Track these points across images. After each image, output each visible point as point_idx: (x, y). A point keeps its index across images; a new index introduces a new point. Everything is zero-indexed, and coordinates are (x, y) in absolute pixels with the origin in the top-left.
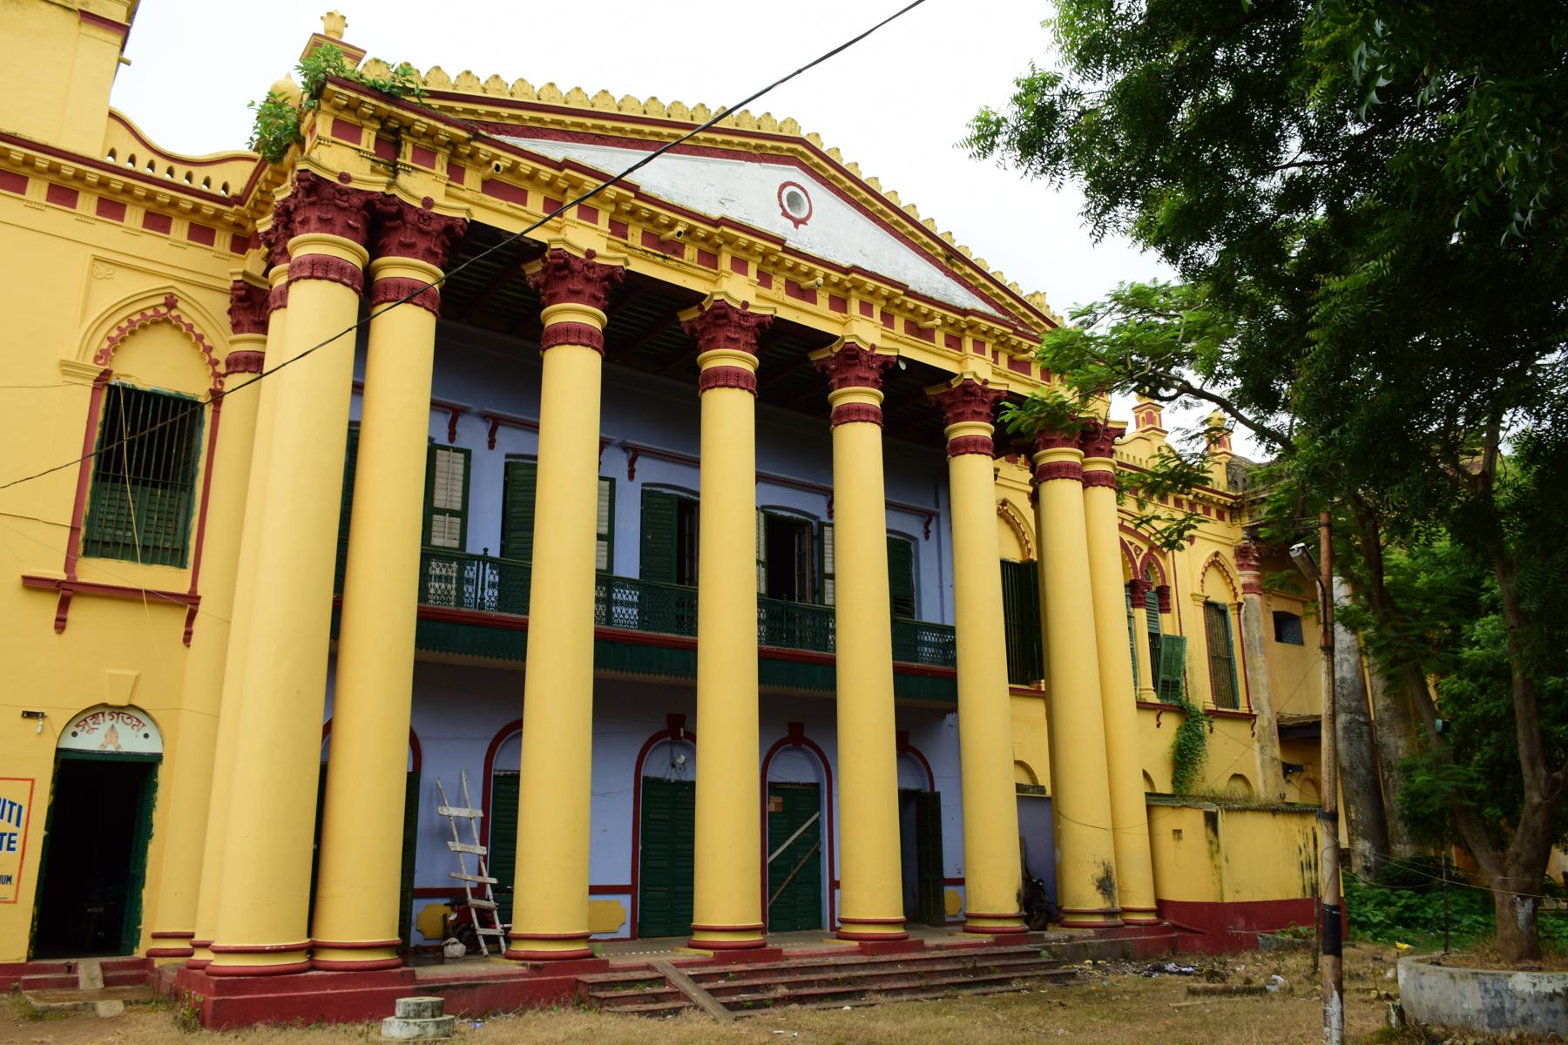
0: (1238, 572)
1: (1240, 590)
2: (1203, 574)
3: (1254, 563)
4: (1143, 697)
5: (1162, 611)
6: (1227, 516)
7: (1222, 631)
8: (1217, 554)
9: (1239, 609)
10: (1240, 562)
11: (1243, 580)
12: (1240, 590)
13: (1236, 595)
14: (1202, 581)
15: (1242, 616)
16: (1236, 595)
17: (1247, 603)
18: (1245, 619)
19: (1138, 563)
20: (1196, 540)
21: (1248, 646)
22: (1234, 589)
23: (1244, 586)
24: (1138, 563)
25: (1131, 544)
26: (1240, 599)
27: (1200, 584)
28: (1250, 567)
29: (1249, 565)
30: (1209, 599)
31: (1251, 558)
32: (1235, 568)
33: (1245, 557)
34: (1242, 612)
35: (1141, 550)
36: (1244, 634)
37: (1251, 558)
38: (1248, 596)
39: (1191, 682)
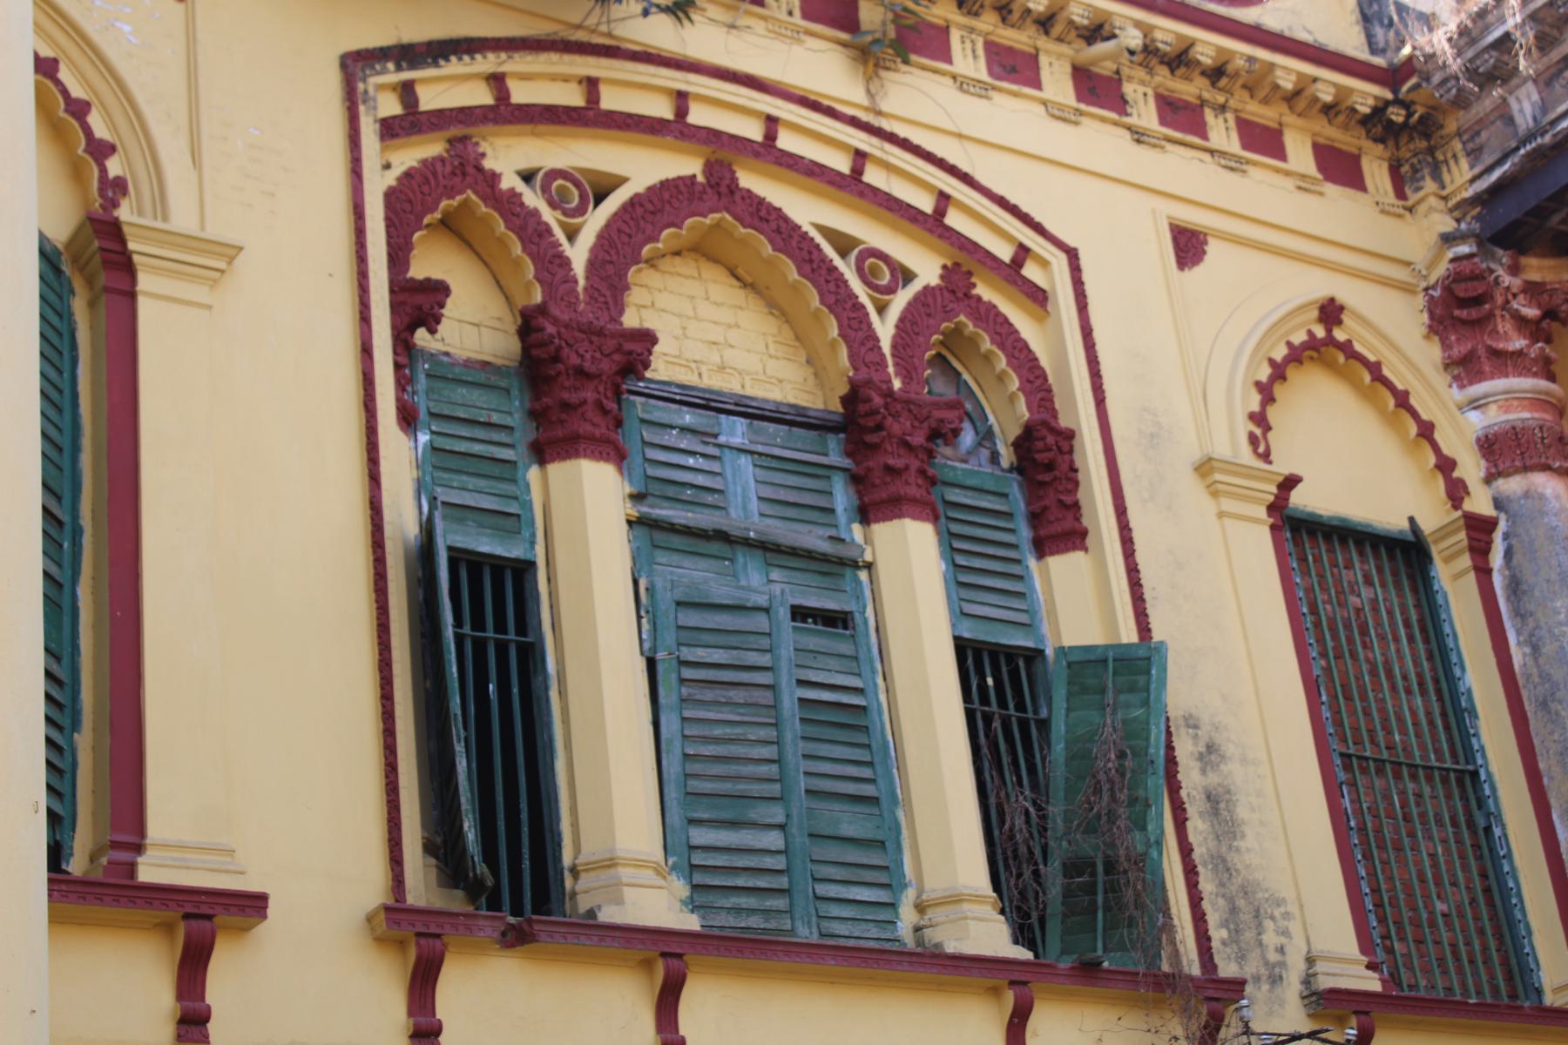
0: (1457, 395)
1: (1471, 468)
2: (1266, 392)
3: (1518, 343)
4: (933, 936)
5: (1043, 547)
6: (1376, 171)
7: (1407, 658)
8: (1331, 312)
9: (1480, 551)
10: (1458, 351)
11: (1477, 421)
12: (1471, 468)
13: (1456, 492)
14: (1259, 419)
15: (1498, 581)
16: (1456, 492)
17: (1513, 518)
18: (1515, 586)
19: (885, 330)
20: (1213, 248)
21: (1544, 705)
22: (1446, 465)
23: (1489, 446)
24: (885, 330)
25: (844, 244)
26: (1480, 502)
27: (1244, 427)
28: (1505, 362)
29: (1496, 354)
30: (1300, 499)
31: (1505, 326)
32: (1440, 380)
33: (1481, 324)
34: (1497, 559)
35: (907, 276)
36: (1518, 655)
37: (1505, 326)
38: (1512, 485)
39: (1223, 867)
